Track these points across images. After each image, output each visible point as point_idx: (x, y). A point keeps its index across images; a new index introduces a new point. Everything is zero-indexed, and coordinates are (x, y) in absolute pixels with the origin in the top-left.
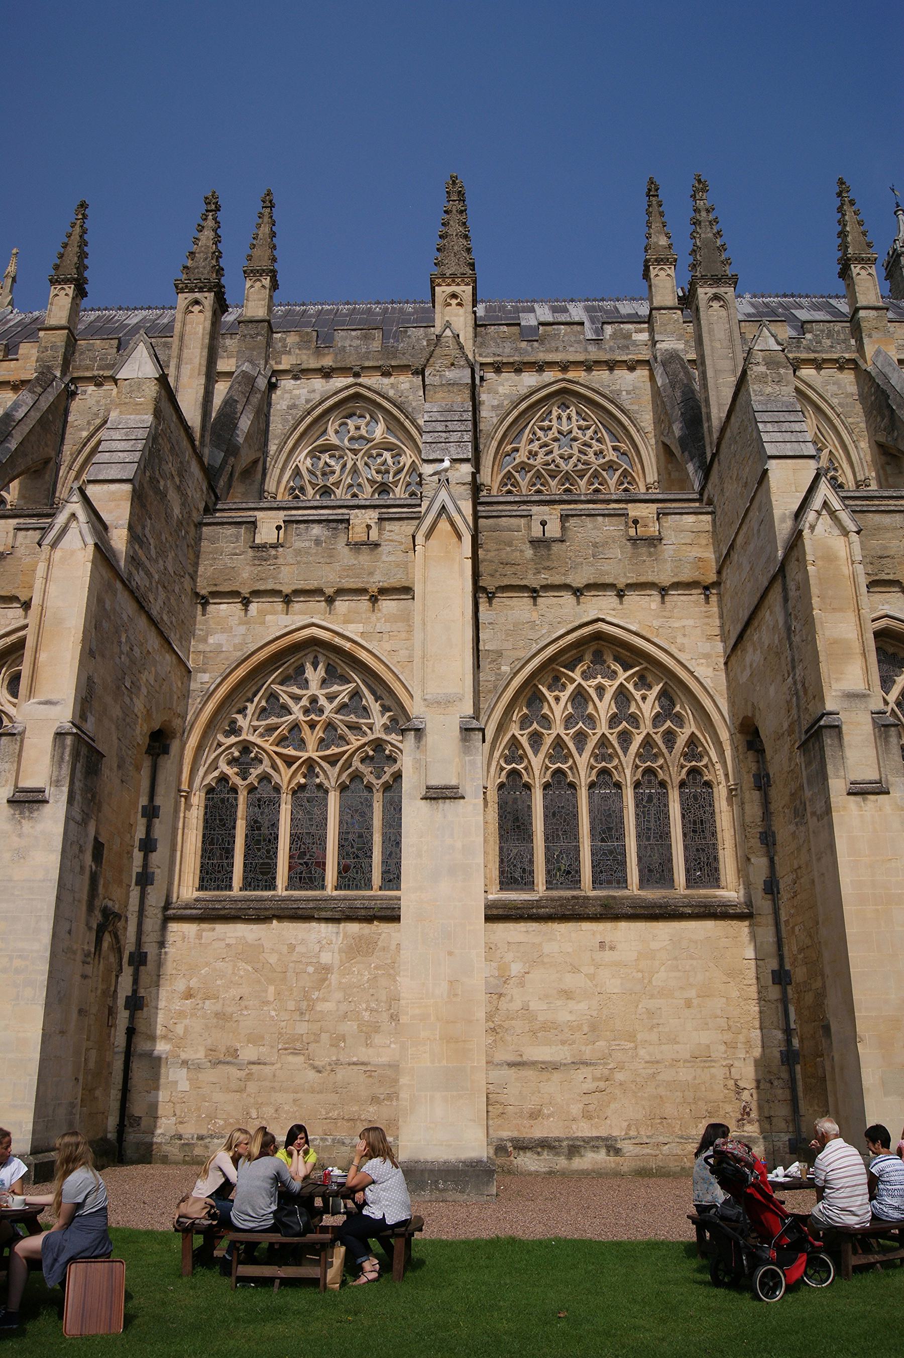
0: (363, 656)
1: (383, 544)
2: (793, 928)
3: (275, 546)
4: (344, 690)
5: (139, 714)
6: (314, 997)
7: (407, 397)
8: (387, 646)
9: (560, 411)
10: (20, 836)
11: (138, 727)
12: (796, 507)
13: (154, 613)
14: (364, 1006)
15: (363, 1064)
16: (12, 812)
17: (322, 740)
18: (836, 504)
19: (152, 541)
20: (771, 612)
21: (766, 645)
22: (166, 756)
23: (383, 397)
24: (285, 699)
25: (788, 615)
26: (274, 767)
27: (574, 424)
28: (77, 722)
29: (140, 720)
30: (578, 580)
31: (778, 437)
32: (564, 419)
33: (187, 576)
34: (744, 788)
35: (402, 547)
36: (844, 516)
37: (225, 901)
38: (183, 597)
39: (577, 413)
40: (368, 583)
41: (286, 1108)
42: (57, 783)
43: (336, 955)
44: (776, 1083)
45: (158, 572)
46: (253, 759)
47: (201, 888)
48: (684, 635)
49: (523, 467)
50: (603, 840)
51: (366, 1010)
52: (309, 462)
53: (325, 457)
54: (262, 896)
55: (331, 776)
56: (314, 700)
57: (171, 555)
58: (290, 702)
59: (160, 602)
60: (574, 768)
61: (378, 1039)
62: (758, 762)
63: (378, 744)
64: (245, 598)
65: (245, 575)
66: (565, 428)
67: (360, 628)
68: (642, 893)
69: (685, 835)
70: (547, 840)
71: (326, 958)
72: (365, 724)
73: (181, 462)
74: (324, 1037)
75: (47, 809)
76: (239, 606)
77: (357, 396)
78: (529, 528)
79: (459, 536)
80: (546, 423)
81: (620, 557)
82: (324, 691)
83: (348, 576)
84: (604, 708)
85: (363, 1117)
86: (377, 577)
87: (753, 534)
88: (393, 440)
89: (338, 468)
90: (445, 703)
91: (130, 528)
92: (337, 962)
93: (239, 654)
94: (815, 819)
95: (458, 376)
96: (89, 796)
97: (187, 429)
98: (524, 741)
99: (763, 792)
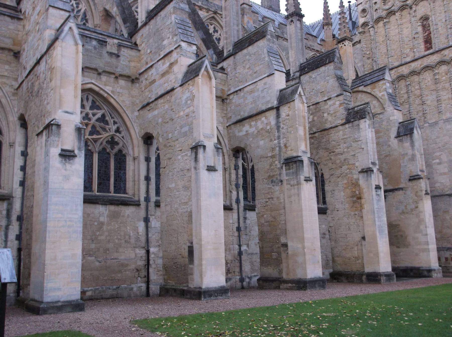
0: (112, 101)
1: (121, 56)
4: (100, 112)
6: (97, 234)
8: (121, 99)
10: (66, 170)
14: (116, 237)
15: (116, 259)
16: (61, 159)
35: (128, 59)
40: (115, 71)
41: (88, 277)
43: (106, 218)
44: (236, 261)
51: (116, 239)
61: (121, 250)
62: (235, 161)
67: (111, 88)
71: (102, 219)
72: (108, 128)
74: (101, 250)
75: (77, 160)
79: (210, 78)
82: (92, 111)
83: (108, 66)
85: (116, 278)
86: (118, 70)
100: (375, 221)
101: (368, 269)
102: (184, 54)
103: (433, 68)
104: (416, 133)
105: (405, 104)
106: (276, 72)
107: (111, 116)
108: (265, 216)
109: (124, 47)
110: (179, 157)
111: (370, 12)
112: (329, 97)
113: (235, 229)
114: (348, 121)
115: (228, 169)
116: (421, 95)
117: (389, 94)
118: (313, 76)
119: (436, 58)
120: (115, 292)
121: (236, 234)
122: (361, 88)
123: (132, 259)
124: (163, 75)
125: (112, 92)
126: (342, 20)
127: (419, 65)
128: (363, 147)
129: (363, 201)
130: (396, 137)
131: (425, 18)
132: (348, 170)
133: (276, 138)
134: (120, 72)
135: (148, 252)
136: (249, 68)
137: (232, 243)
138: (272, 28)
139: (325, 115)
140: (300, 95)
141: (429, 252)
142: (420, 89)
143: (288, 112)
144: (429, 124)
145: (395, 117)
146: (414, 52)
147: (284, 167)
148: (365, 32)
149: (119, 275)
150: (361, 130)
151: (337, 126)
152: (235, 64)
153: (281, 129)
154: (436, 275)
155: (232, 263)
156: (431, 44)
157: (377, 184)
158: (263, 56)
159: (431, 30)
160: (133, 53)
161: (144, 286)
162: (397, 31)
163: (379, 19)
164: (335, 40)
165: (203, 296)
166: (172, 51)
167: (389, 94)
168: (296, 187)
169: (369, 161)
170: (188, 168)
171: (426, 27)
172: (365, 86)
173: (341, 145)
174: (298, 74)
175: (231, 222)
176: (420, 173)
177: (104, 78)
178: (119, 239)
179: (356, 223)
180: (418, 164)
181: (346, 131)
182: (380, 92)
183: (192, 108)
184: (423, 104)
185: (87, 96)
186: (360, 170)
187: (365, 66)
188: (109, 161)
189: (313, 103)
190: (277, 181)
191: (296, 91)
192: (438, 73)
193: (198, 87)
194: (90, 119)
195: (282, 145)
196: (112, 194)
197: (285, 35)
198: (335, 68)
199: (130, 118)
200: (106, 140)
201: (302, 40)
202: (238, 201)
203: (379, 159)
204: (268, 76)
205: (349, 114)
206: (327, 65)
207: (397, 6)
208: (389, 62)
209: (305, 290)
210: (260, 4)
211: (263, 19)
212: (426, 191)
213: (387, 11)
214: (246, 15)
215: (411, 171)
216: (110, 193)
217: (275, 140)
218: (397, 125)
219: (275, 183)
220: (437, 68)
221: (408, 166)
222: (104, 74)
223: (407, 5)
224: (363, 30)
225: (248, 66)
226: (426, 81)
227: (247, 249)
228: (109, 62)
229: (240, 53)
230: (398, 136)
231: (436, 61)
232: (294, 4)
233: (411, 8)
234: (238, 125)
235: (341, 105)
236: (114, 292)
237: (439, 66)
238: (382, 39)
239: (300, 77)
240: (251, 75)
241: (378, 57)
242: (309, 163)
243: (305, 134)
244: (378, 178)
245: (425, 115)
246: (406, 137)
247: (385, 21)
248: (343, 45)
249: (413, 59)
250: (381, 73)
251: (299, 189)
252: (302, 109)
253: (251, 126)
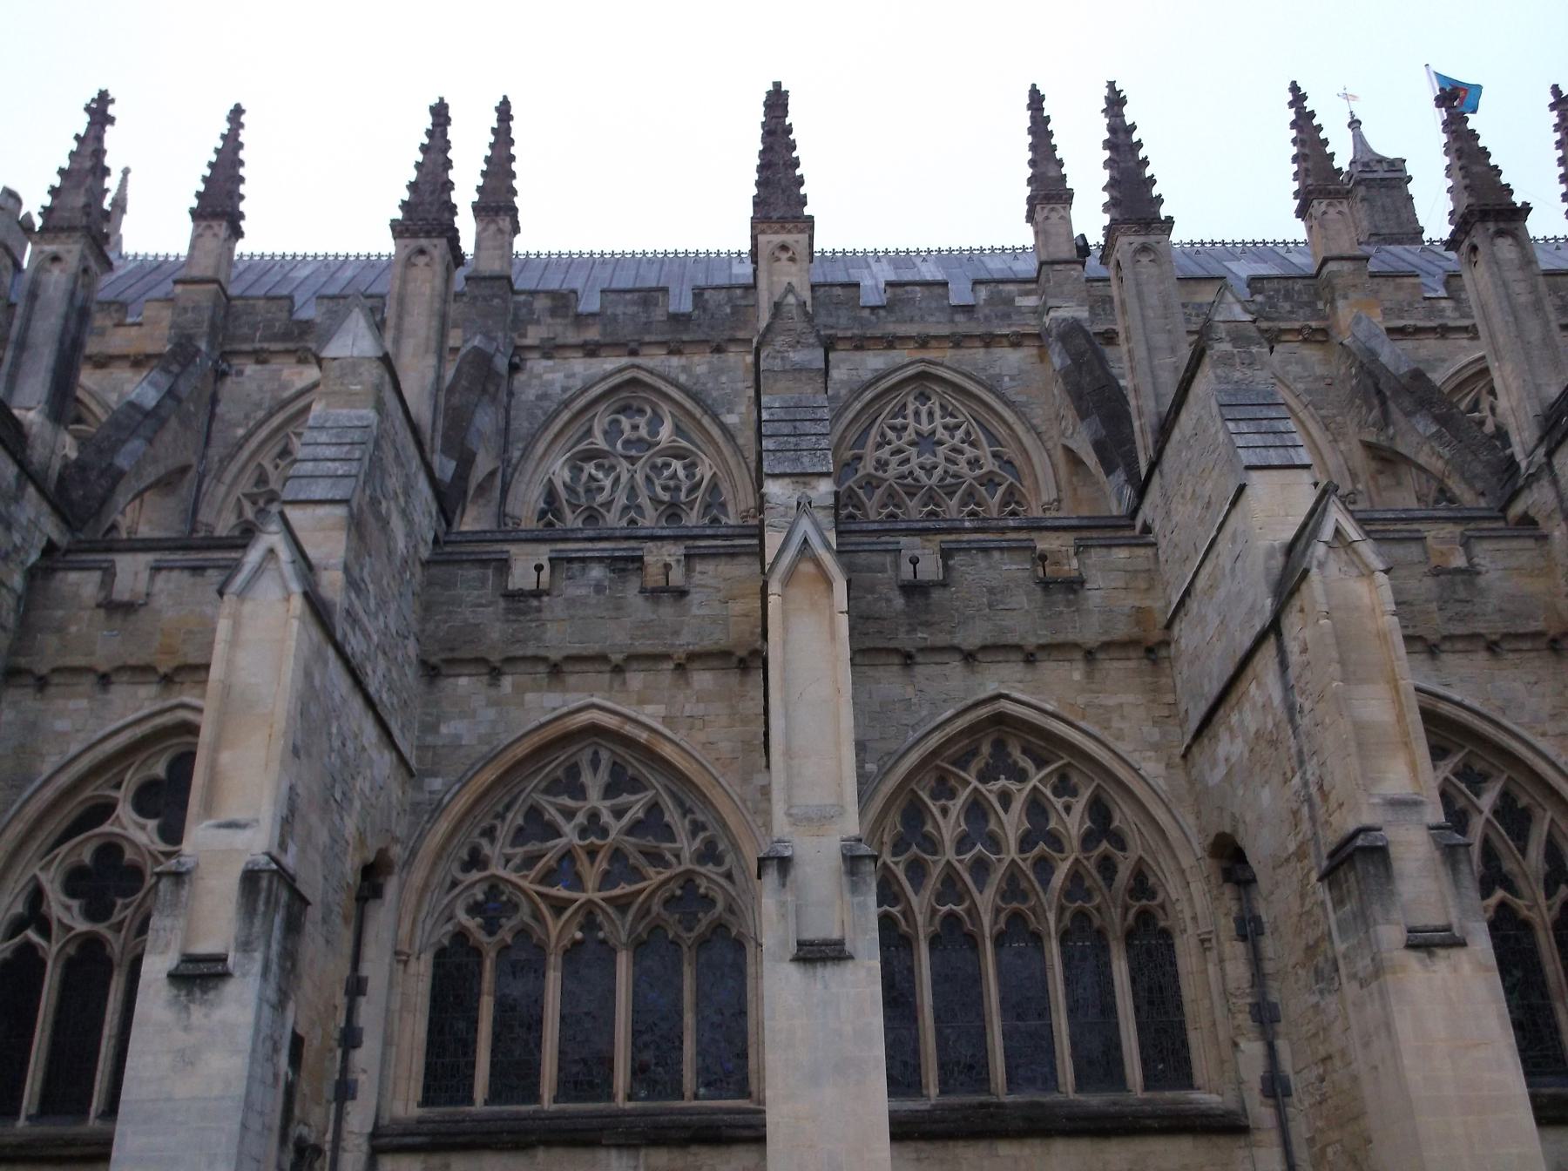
0: (667, 751)
1: (693, 590)
2: (1323, 1150)
3: (538, 594)
4: (637, 801)
5: (351, 841)
7: (704, 384)
8: (701, 737)
9: (918, 404)
10: (186, 1029)
11: (349, 858)
12: (1289, 535)
13: (372, 690)
16: (175, 992)
17: (606, 874)
18: (1352, 532)
19: (371, 587)
20: (1259, 685)
21: (1253, 729)
22: (378, 901)
23: (672, 384)
24: (551, 813)
25: (1288, 689)
26: (537, 916)
27: (938, 421)
28: (275, 852)
29: (351, 849)
30: (971, 638)
31: (1257, 440)
32: (924, 417)
33: (412, 638)
34: (1222, 938)
35: (720, 595)
36: (1367, 549)
37: (464, 1121)
38: (407, 667)
39: (942, 407)
40: (672, 645)
42: (245, 946)
45: (377, 632)
46: (505, 903)
47: (426, 1102)
48: (1123, 717)
49: (870, 484)
50: (1019, 1017)
52: (567, 475)
53: (590, 468)
54: (518, 1113)
55: (619, 930)
56: (594, 816)
57: (393, 606)
58: (560, 819)
59: (380, 673)
60: (973, 911)
62: (1239, 899)
63: (688, 879)
64: (494, 669)
65: (495, 636)
66: (925, 427)
67: (660, 709)
68: (1082, 1098)
69: (1137, 1009)
70: (937, 1019)
72: (670, 850)
73: (407, 475)
75: (231, 988)
76: (485, 679)
77: (634, 383)
78: (897, 566)
79: (829, 583)
80: (899, 421)
81: (1026, 607)
82: (608, 803)
83: (643, 636)
84: (1012, 824)
86: (683, 639)
87: (1224, 575)
88: (684, 444)
89: (608, 483)
90: (818, 820)
91: (346, 569)
93: (486, 748)
94: (1355, 985)
95: (808, 358)
96: (289, 965)
97: (415, 429)
98: (900, 872)
99: (1250, 945)
109: (703, 556)
125: (666, 720)
134: (688, 644)
153: (1298, 716)
185: (596, 753)
194: (604, 832)
196: (1072, 1096)
199: (736, 798)
200: (663, 894)
211: (1446, 285)
214: (1345, 297)
216: (682, 1097)
222: (635, 665)
228: (652, 621)
234: (1206, 741)
239: (1549, 464)
252: (1367, 600)
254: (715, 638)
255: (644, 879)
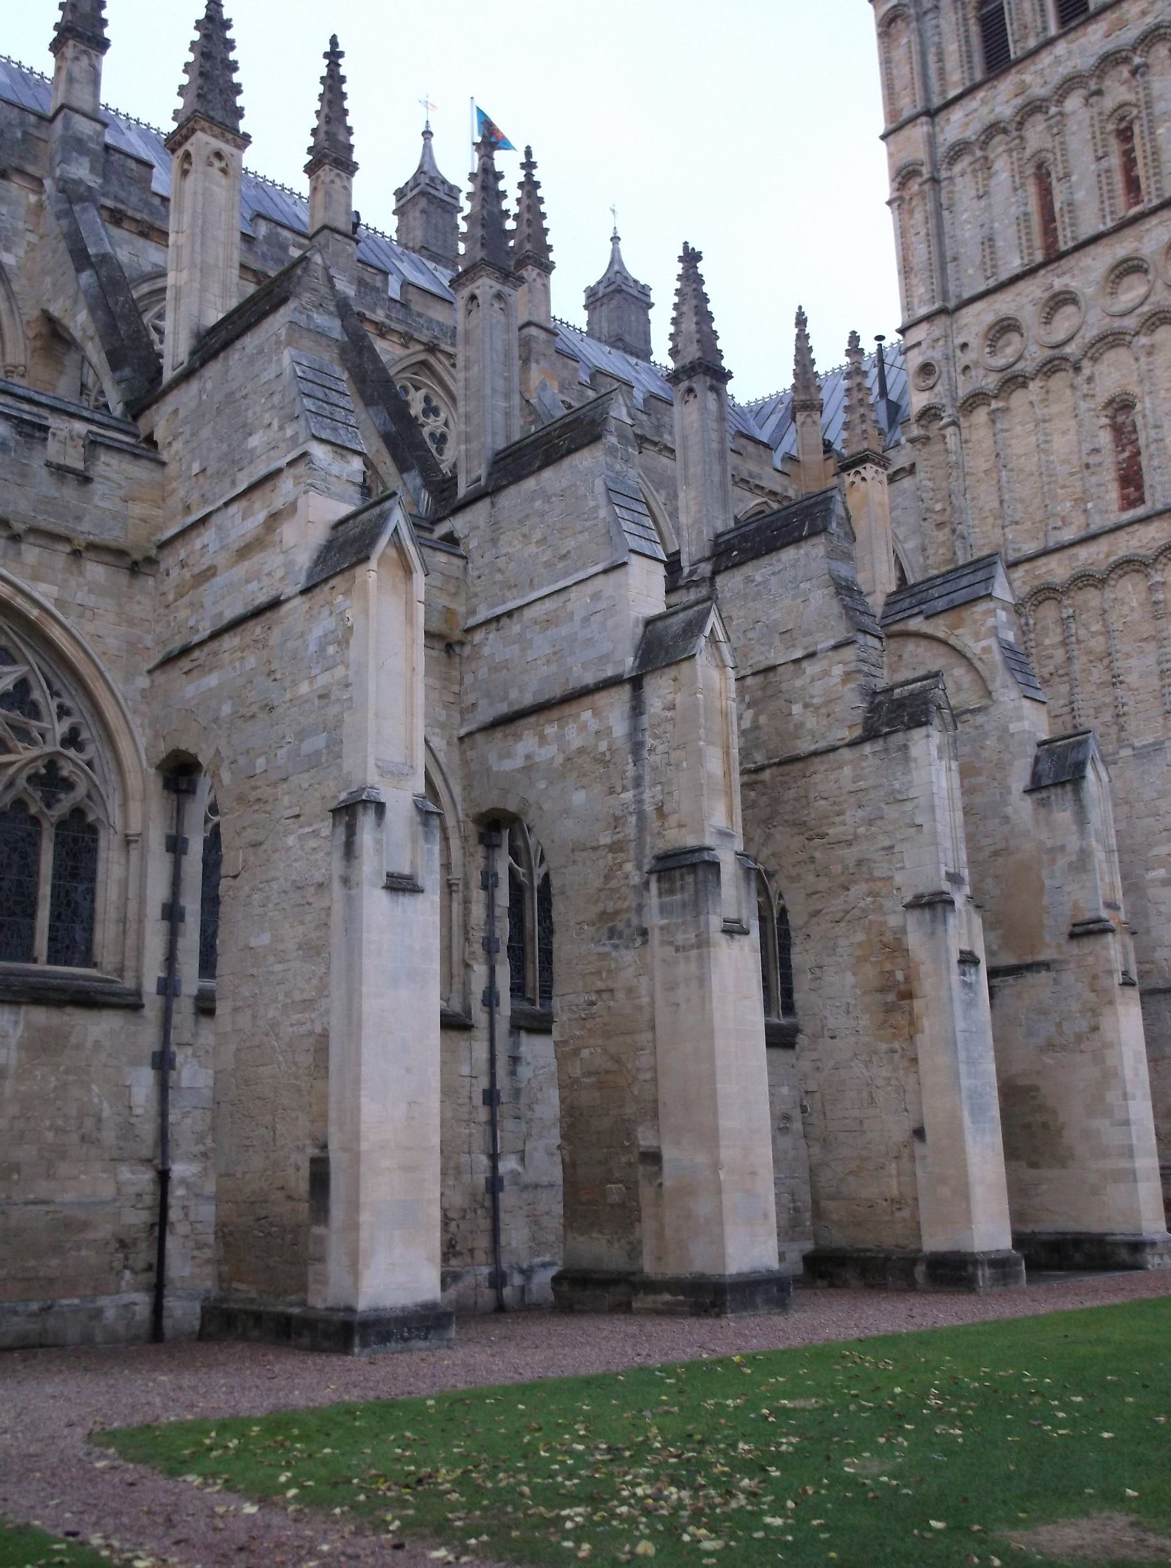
0: (56, 633)
1: (96, 479)
8: (90, 627)
14: (48, 1123)
15: (44, 1202)
35: (122, 492)
40: (74, 530)
43: (14, 1054)
44: (479, 1212)
51: (50, 1129)
61: (63, 1169)
62: (487, 858)
72: (38, 728)
79: (408, 571)
83: (46, 512)
85: (41, 1274)
86: (85, 526)
92: (13, 1062)
95: (327, 324)
100: (957, 1075)
101: (934, 1242)
102: (319, 483)
103: (1147, 566)
104: (1094, 779)
105: (1057, 679)
106: (634, 560)
107: (49, 686)
108: (585, 1053)
109: (109, 447)
110: (291, 841)
111: (945, 375)
112: (811, 650)
113: (478, 1099)
114: (870, 734)
115: (461, 887)
116: (1110, 654)
117: (1006, 647)
118: (758, 578)
119: (1158, 536)
120: (34, 1326)
121: (483, 1115)
122: (916, 624)
123: (104, 1203)
124: (244, 552)
125: (59, 602)
126: (857, 395)
127: (1102, 556)
128: (918, 821)
129: (918, 1004)
130: (1027, 792)
131: (1122, 405)
132: (869, 899)
133: (628, 783)
135: (163, 1177)
136: (542, 541)
137: (466, 1148)
138: (624, 411)
139: (796, 709)
140: (713, 640)
141: (1135, 1181)
142: (1107, 633)
143: (670, 697)
144: (1134, 749)
145: (1026, 725)
146: (1085, 511)
147: (654, 886)
148: (928, 438)
149: (54, 1262)
150: (913, 765)
151: (834, 749)
152: (495, 525)
154: (1157, 1260)
155: (464, 1218)
156: (1139, 487)
157: (966, 948)
158: (592, 504)
159: (1142, 442)
160: (140, 471)
161: (142, 1302)
162: (1033, 439)
163: (976, 399)
164: (831, 462)
165: (357, 1340)
166: (279, 471)
167: (1006, 647)
168: (694, 953)
169: (938, 869)
170: (321, 880)
171: (1123, 434)
172: (927, 618)
173: (848, 813)
174: (706, 569)
175: (465, 1070)
176: (1104, 914)
177: (31, 553)
178: (58, 1131)
179: (894, 1082)
180: (1099, 883)
181: (864, 764)
182: (978, 640)
183: (339, 671)
184: (1114, 684)
186: (908, 899)
187: (930, 552)
188: (36, 845)
189: (756, 669)
190: (626, 932)
191: (701, 629)
192: (1164, 583)
193: (366, 599)
195: (649, 808)
197: (666, 436)
198: (831, 555)
199: (119, 695)
201: (722, 456)
202: (490, 999)
203: (972, 863)
204: (605, 572)
205: (874, 709)
206: (803, 543)
207: (1033, 359)
208: (1006, 540)
209: (718, 1316)
210: (585, 329)
211: (593, 377)
212: (1125, 973)
213: (1000, 375)
214: (537, 362)
215: (1076, 905)
216: (35, 961)
217: (624, 789)
218: (1032, 750)
219: (620, 937)
220: (1159, 567)
221: (1067, 889)
222: (32, 539)
223: (1065, 359)
224: (922, 432)
225: (537, 535)
226: (1125, 610)
227: (520, 1169)
229: (512, 490)
230: (1036, 786)
231: (1156, 545)
232: (697, 336)
233: (1077, 369)
235: (848, 676)
236: (31, 1326)
237: (1165, 561)
238: (985, 466)
239: (712, 579)
240: (549, 565)
241: (971, 523)
242: (740, 873)
243: (727, 774)
244: (970, 931)
245: (1122, 720)
246: (1059, 791)
247: (994, 405)
248: (857, 479)
249: (1083, 534)
250: (980, 576)
251: (703, 962)
253: (543, 739)
254: (113, 536)
255: (8, 751)
